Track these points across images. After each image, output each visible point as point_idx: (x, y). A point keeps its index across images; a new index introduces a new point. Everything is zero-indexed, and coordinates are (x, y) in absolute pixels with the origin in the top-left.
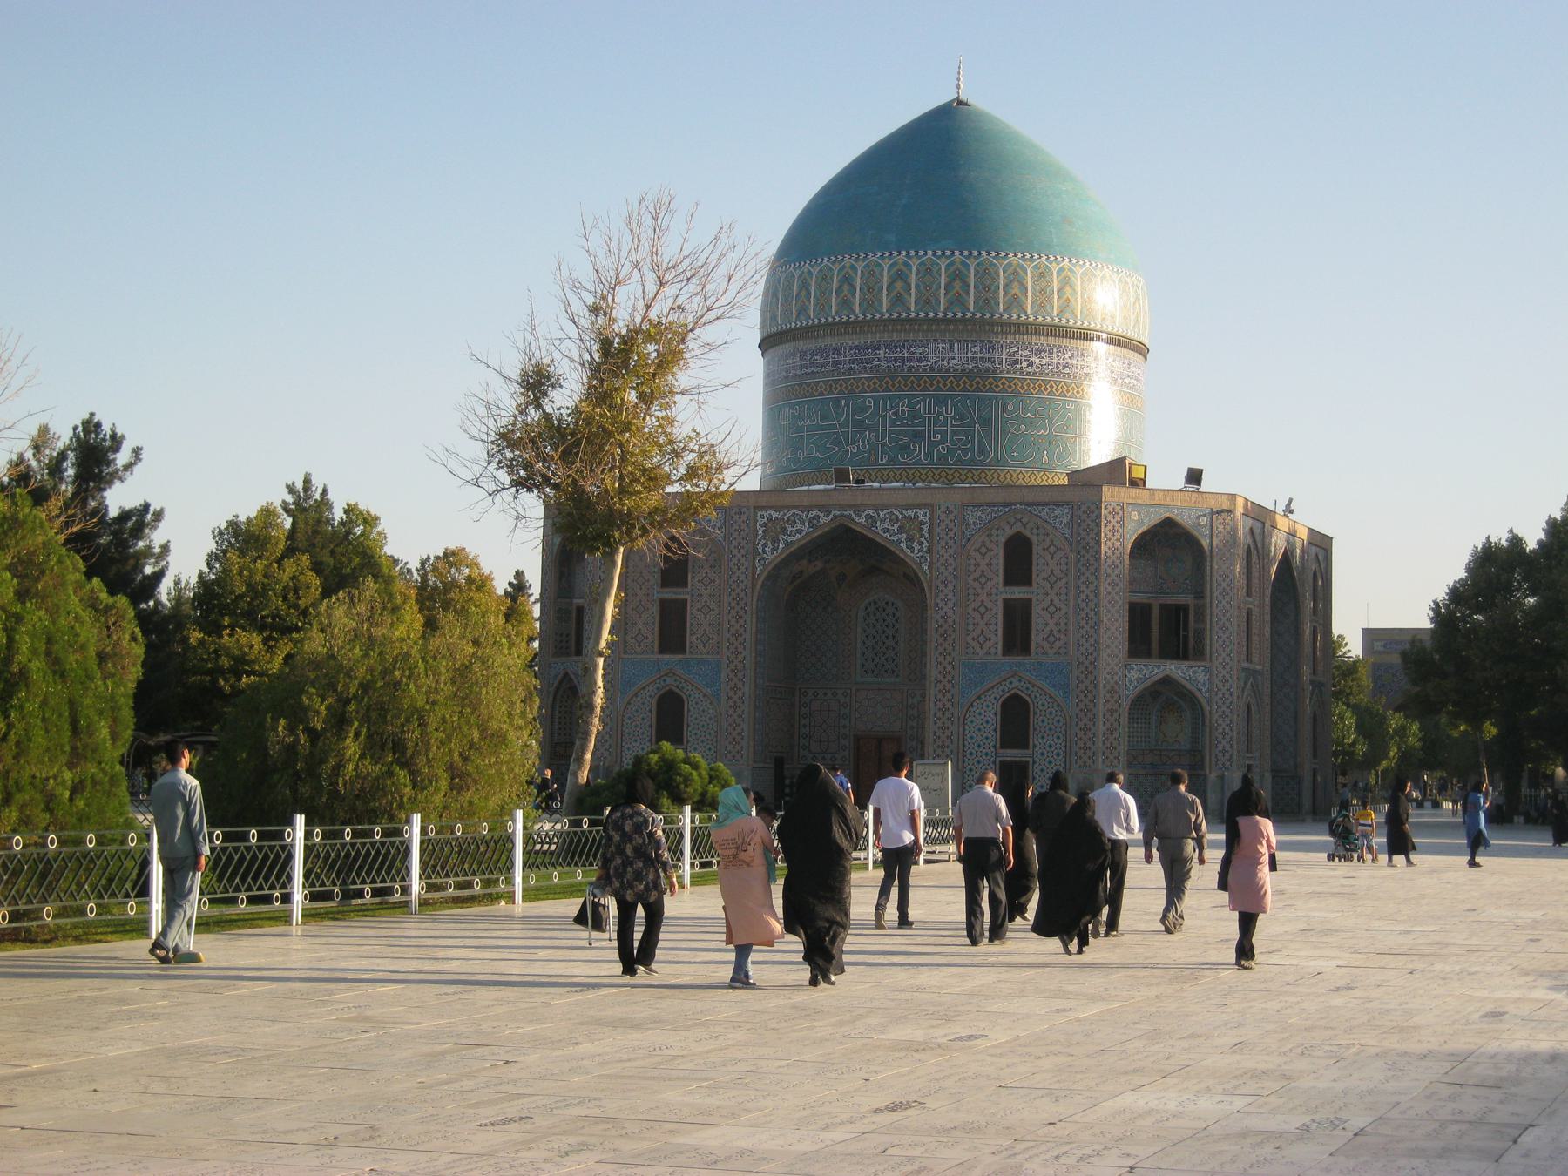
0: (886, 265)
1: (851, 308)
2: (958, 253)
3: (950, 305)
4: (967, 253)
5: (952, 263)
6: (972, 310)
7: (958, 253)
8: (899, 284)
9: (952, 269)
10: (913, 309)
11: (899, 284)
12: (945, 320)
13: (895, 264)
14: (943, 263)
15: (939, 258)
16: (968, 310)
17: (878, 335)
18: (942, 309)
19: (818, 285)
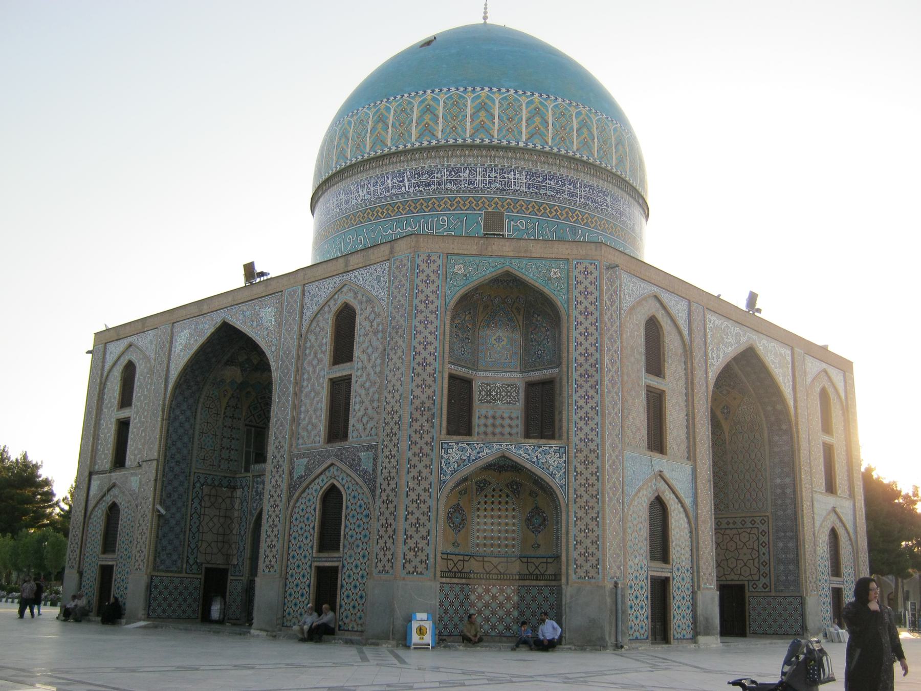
0: (469, 98)
1: (433, 135)
2: (537, 95)
3: (531, 137)
4: (545, 96)
5: (532, 102)
6: (550, 144)
7: (537, 95)
8: (482, 114)
9: (533, 106)
10: (496, 136)
11: (482, 114)
12: (524, 150)
13: (478, 97)
14: (524, 100)
15: (520, 96)
16: (547, 144)
17: (454, 160)
18: (524, 138)
19: (396, 117)
